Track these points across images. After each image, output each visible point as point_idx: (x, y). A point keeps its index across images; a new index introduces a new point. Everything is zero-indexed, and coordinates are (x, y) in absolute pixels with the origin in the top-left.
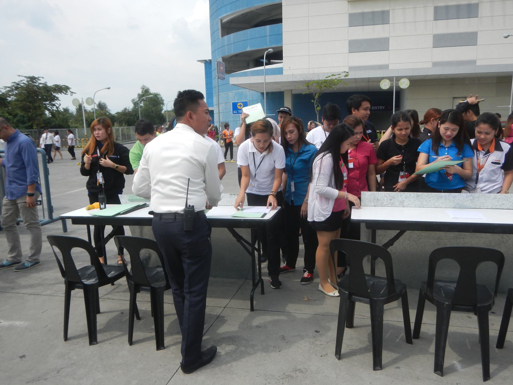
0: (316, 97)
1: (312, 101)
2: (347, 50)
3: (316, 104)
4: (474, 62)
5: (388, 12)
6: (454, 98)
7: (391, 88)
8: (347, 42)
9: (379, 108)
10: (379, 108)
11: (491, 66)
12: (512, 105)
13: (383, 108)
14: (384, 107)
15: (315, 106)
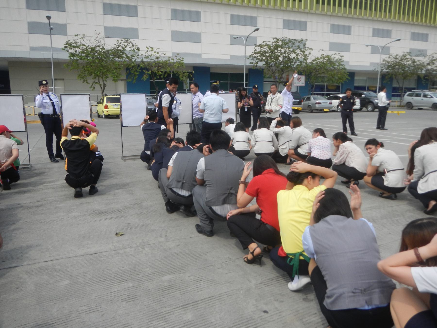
12: (54, 86)
13: (2, 86)
14: (4, 85)
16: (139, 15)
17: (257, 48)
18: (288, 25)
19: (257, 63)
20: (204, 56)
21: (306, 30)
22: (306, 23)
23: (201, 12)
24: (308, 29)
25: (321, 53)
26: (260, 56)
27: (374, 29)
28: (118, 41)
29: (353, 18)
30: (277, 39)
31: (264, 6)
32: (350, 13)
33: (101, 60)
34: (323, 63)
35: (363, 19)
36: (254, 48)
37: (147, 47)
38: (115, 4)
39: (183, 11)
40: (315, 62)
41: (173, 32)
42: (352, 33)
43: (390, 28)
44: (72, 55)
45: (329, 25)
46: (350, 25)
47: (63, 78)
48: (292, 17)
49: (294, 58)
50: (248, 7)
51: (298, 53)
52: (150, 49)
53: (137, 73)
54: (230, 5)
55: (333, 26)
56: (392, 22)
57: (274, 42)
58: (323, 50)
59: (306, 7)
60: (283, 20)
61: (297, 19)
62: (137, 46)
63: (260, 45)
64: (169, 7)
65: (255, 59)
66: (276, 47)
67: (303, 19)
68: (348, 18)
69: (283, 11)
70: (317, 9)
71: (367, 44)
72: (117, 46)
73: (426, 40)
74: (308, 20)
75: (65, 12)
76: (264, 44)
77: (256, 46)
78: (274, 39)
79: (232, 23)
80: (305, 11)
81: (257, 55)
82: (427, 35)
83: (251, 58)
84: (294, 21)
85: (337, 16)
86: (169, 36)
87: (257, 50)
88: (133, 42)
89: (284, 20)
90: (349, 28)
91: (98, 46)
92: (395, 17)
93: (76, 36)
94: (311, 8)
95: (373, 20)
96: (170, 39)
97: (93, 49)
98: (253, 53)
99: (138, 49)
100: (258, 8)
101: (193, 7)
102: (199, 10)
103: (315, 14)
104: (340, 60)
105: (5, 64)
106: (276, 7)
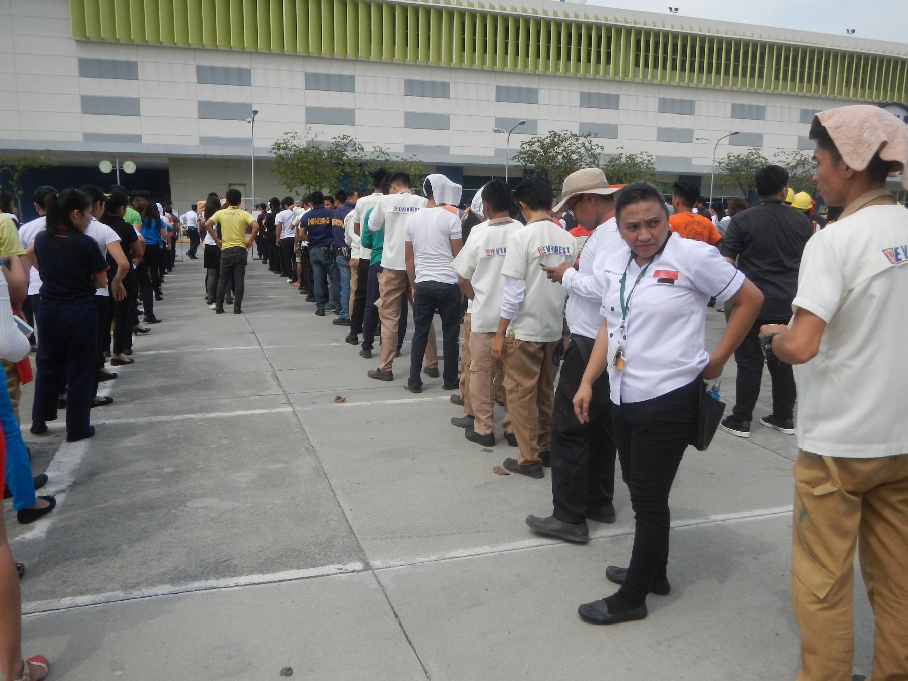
0: (15, 177)
1: (10, 182)
2: (79, 109)
3: (15, 187)
4: (248, 142)
5: (135, 64)
7: (114, 171)
8: (78, 98)
9: (142, 192)
10: (142, 192)
12: (254, 197)
13: (147, 193)
15: (15, 189)
16: (356, 90)
18: (588, 101)
20: (454, 151)
21: (618, 109)
22: (618, 97)
23: (449, 83)
24: (620, 108)
25: (620, 151)
26: (528, 157)
27: (734, 106)
28: (335, 138)
29: (697, 88)
30: (555, 134)
31: (548, 73)
32: (691, 80)
33: (315, 163)
34: (624, 165)
35: (714, 90)
37: (374, 147)
39: (423, 83)
41: (407, 115)
43: (762, 104)
44: (281, 156)
45: (658, 100)
46: (694, 99)
47: (243, 183)
48: (595, 89)
49: (577, 159)
50: (523, 74)
51: (582, 152)
52: (378, 149)
53: (361, 183)
54: (496, 72)
56: (765, 94)
57: (547, 138)
58: (622, 148)
59: (616, 73)
63: (530, 142)
64: (402, 77)
65: (522, 161)
66: (553, 144)
69: (580, 78)
70: (635, 74)
71: (698, 137)
72: (336, 146)
75: (251, 86)
76: (536, 140)
77: (523, 144)
79: (499, 99)
80: (616, 79)
81: (524, 156)
84: (599, 95)
85: (669, 86)
87: (525, 148)
88: (356, 141)
89: (582, 94)
90: (691, 104)
91: (313, 147)
92: (768, 86)
93: (285, 134)
95: (732, 91)
96: (402, 125)
97: (307, 152)
99: (362, 149)
100: (539, 75)
101: (439, 77)
102: (448, 80)
103: (633, 82)
104: (649, 161)
105: (165, 161)
106: (568, 75)
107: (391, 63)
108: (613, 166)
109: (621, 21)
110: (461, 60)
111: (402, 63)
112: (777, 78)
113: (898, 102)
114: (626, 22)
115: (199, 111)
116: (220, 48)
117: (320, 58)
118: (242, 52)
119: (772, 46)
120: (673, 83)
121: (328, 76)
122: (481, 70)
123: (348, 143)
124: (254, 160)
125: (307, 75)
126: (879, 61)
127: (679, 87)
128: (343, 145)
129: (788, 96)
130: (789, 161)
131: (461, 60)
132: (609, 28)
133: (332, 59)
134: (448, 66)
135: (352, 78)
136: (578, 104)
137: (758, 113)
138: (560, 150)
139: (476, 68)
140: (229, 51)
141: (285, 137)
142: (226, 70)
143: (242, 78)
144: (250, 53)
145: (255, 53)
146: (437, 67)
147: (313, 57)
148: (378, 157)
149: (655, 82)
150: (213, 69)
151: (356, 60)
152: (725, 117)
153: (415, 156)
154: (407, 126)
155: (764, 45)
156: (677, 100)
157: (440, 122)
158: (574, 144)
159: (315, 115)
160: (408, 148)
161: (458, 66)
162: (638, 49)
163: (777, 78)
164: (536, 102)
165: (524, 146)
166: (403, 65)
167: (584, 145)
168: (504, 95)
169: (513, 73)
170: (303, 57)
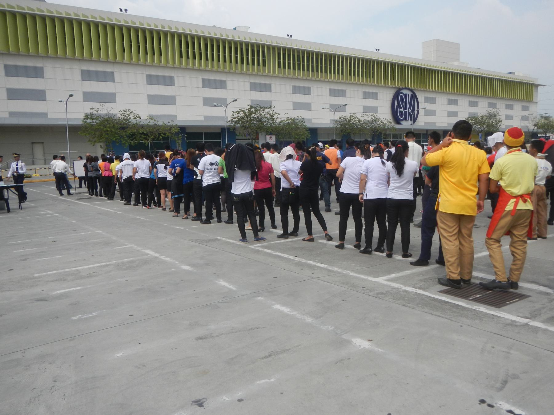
4: (45, 115)
6: (33, 143)
11: (58, 119)
17: (234, 114)
18: (254, 87)
19: (235, 125)
20: (179, 118)
22: (270, 85)
23: (174, 77)
25: (287, 116)
27: (330, 90)
28: (121, 111)
29: (311, 80)
31: (231, 71)
35: (320, 81)
36: (233, 114)
38: (93, 71)
39: (157, 76)
40: (282, 124)
42: (312, 93)
43: (344, 89)
45: (291, 86)
46: (310, 86)
48: (258, 80)
50: (217, 72)
55: (294, 88)
56: (345, 83)
58: (287, 114)
59: (269, 72)
60: (249, 83)
61: (263, 82)
62: (137, 114)
63: (237, 111)
64: (144, 73)
67: (267, 82)
68: (307, 80)
71: (323, 107)
73: (377, 99)
74: (272, 83)
75: (44, 78)
77: (233, 113)
78: (248, 106)
79: (204, 87)
82: (376, 94)
83: (231, 122)
84: (260, 84)
85: (297, 79)
86: (145, 100)
87: (234, 115)
88: (134, 112)
89: (251, 83)
90: (309, 88)
94: (274, 72)
95: (329, 82)
96: (147, 102)
98: (232, 118)
101: (167, 73)
102: (173, 75)
103: (278, 77)
104: (302, 121)
106: (243, 72)
107: (137, 64)
108: (284, 124)
109: (275, 43)
110: (181, 63)
111: (144, 64)
112: (350, 75)
113: (408, 87)
114: (272, 43)
115: (8, 95)
116: (21, 53)
117: (91, 60)
118: (37, 56)
119: (347, 57)
120: (299, 77)
121: (97, 72)
122: (193, 69)
123: (129, 114)
124: (68, 127)
125: (83, 72)
126: (407, 67)
127: (302, 79)
128: (127, 115)
129: (353, 84)
130: (369, 119)
131: (181, 63)
132: (263, 46)
133: (99, 61)
134: (173, 66)
135: (113, 73)
136: (249, 89)
137: (342, 94)
138: (256, 116)
139: (197, 68)
140: (28, 55)
141: (91, 111)
142: (26, 67)
143: (38, 73)
144: (43, 57)
145: (46, 57)
146: (166, 67)
147: (86, 60)
148: (149, 123)
149: (290, 76)
150: (16, 67)
151: (115, 62)
152: (326, 96)
153: (173, 121)
154: (150, 102)
155: (343, 57)
156: (301, 87)
157: (170, 100)
158: (263, 113)
159: (88, 97)
160: (151, 117)
161: (179, 67)
162: (279, 58)
163: (350, 75)
164: (225, 88)
165: (234, 114)
166: (145, 65)
167: (268, 112)
168: (207, 84)
169: (212, 71)
170: (79, 60)
